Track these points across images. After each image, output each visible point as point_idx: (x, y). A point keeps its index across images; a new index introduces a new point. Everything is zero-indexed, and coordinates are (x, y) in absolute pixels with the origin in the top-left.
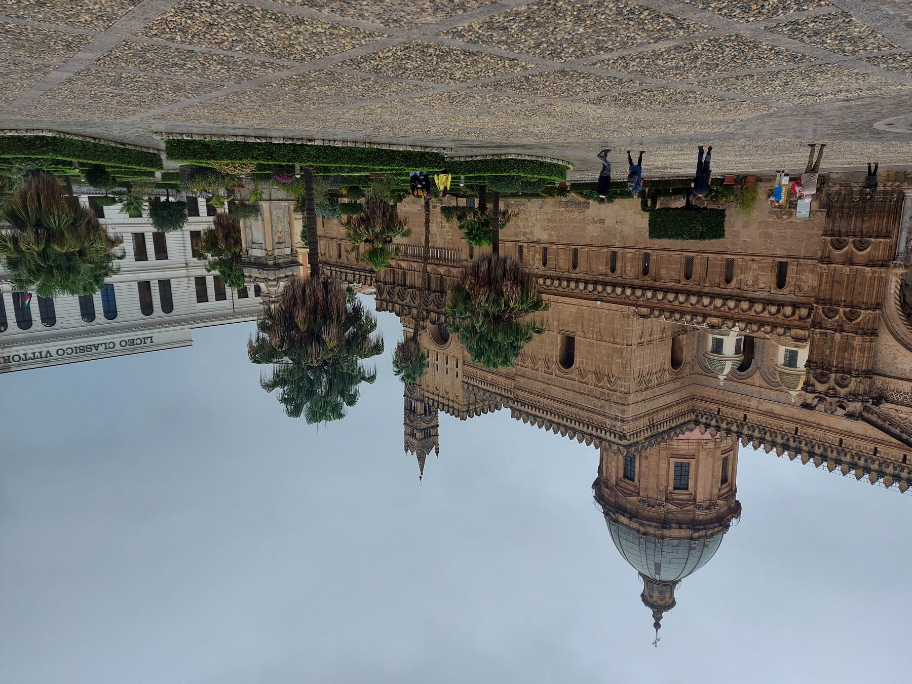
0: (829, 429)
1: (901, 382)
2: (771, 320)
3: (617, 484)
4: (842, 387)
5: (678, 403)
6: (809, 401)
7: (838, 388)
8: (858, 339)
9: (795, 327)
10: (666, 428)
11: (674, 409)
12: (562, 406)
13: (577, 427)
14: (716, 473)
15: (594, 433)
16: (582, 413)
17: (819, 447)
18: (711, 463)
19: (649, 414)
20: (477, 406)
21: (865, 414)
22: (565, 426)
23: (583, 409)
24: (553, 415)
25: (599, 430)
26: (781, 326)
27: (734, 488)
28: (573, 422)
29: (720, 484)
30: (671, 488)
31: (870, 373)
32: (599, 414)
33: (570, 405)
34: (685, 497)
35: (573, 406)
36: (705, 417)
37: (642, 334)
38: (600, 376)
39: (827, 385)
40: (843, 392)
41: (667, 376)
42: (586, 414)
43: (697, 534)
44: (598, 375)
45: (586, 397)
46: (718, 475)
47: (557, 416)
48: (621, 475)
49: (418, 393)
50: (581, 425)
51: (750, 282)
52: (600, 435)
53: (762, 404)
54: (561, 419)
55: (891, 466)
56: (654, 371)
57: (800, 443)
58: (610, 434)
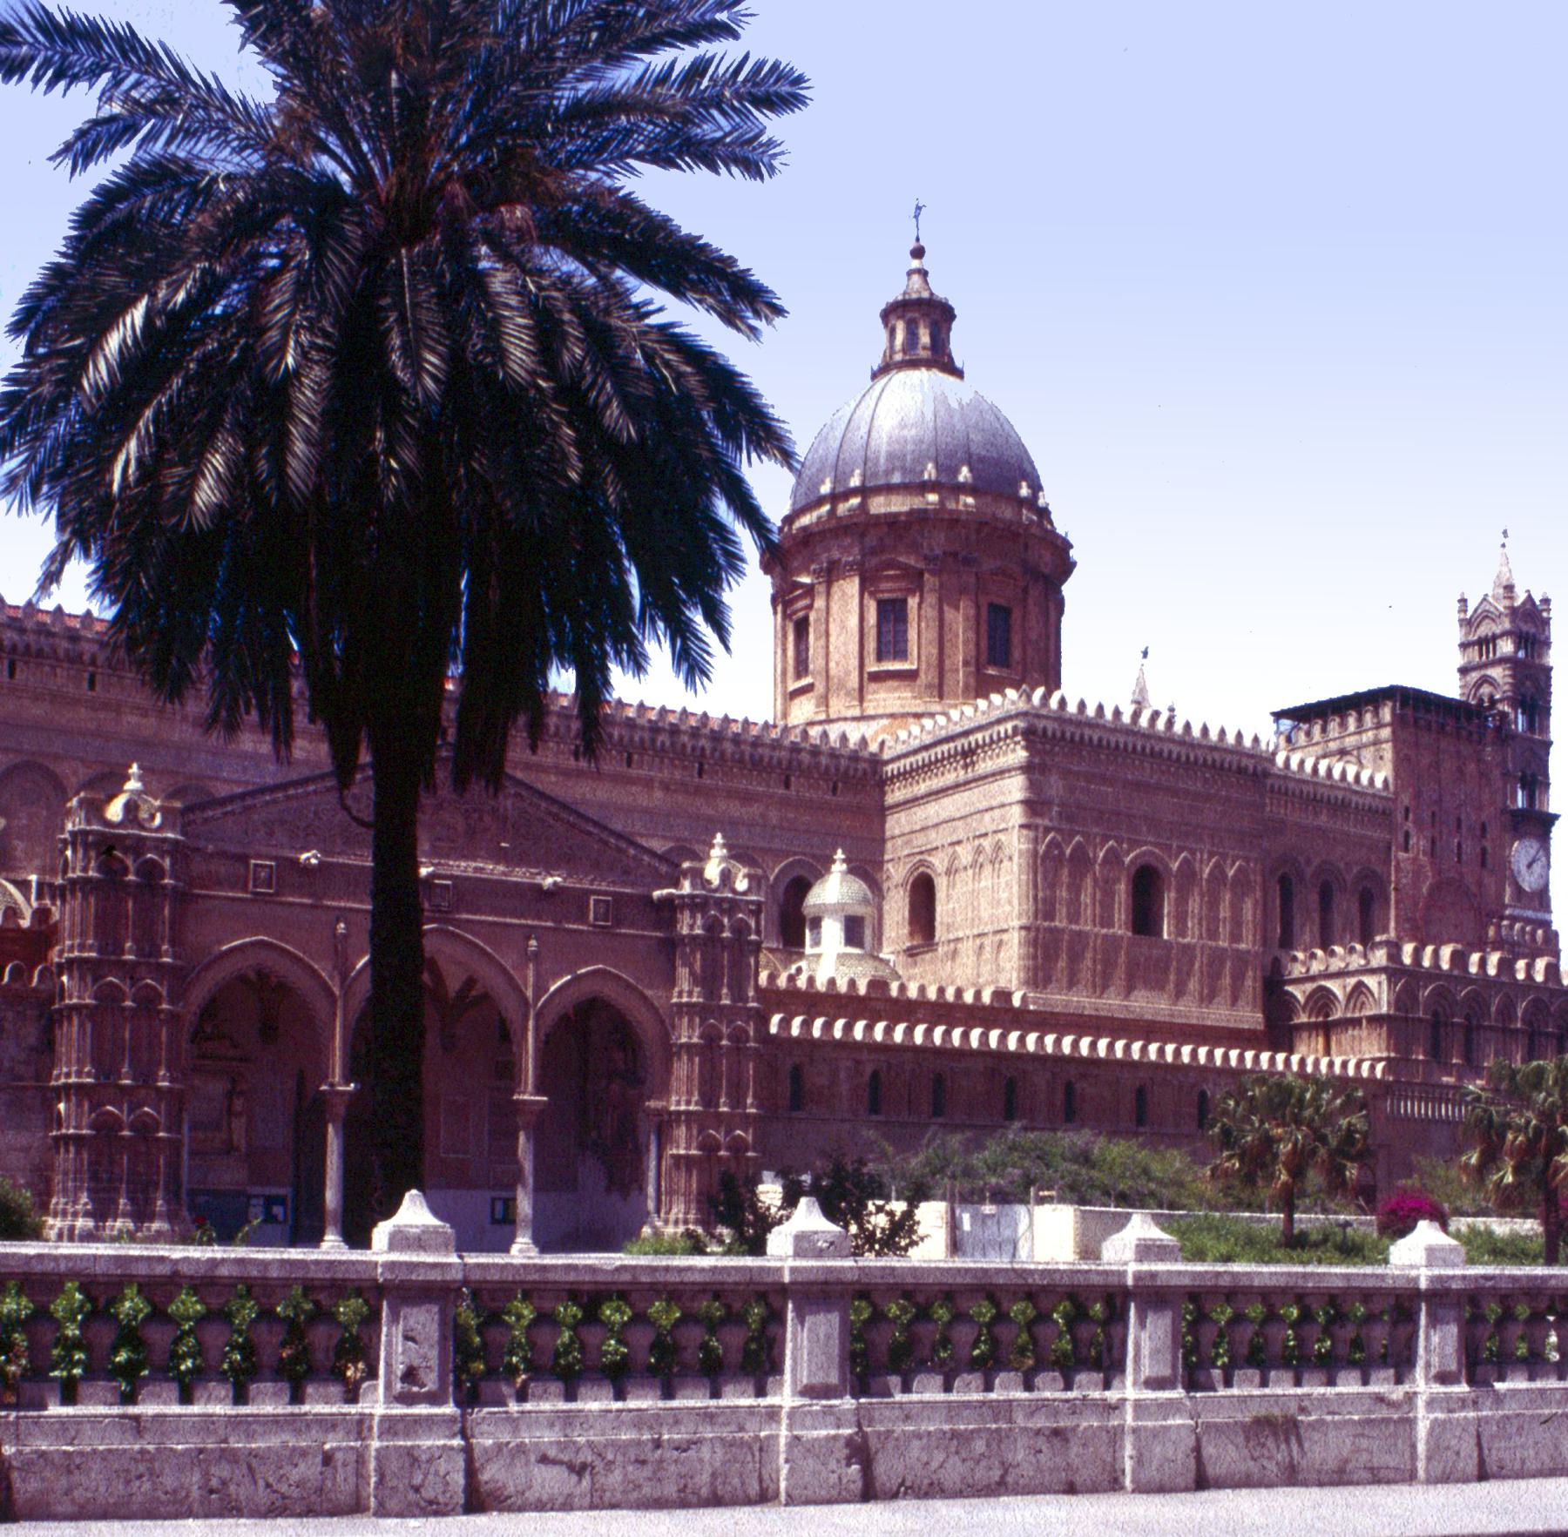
0: (648, 783)
3: (1025, 591)
5: (914, 801)
10: (939, 749)
11: (922, 788)
14: (822, 642)
17: (663, 744)
18: (832, 665)
19: (975, 780)
27: (779, 608)
29: (812, 618)
30: (913, 602)
34: (884, 586)
36: (860, 773)
37: (998, 951)
43: (855, 501)
46: (816, 639)
48: (1016, 615)
51: (843, 1075)
53: (762, 816)
56: (970, 872)
57: (694, 749)
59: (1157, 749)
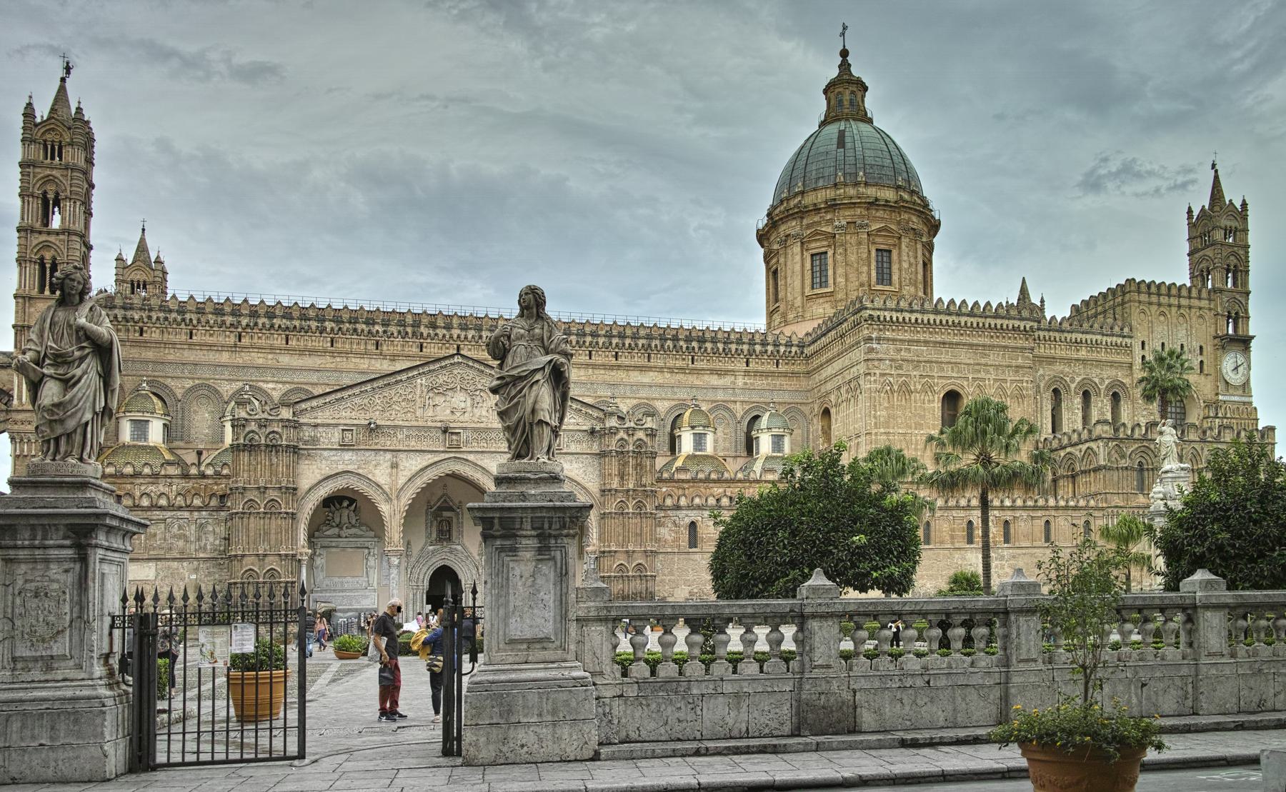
1: (578, 451)
2: (711, 485)
4: (622, 439)
6: (649, 419)
7: (625, 437)
8: (614, 486)
9: (687, 481)
12: (957, 339)
13: (932, 317)
15: (907, 315)
16: (927, 337)
20: (1112, 303)
21: (601, 415)
22: (950, 314)
23: (926, 342)
24: (969, 325)
25: (901, 320)
26: (701, 481)
28: (938, 322)
31: (602, 455)
32: (901, 340)
33: (944, 343)
35: (940, 343)
38: (904, 389)
39: (635, 438)
40: (622, 434)
41: (833, 398)
42: (921, 337)
44: (906, 390)
45: (921, 359)
47: (963, 324)
49: (1221, 304)
50: (926, 322)
52: (899, 314)
54: (956, 321)
55: (601, 344)
58: (885, 319)
59: (956, 321)
